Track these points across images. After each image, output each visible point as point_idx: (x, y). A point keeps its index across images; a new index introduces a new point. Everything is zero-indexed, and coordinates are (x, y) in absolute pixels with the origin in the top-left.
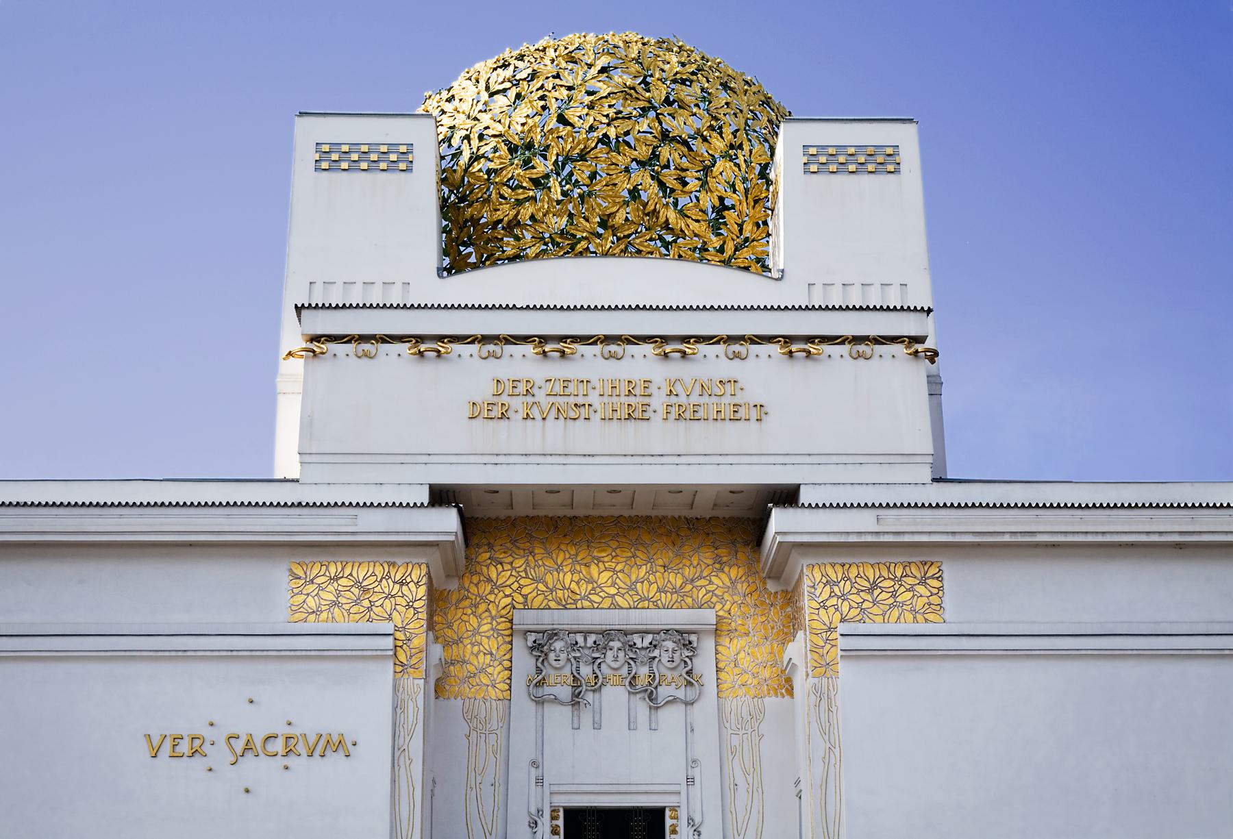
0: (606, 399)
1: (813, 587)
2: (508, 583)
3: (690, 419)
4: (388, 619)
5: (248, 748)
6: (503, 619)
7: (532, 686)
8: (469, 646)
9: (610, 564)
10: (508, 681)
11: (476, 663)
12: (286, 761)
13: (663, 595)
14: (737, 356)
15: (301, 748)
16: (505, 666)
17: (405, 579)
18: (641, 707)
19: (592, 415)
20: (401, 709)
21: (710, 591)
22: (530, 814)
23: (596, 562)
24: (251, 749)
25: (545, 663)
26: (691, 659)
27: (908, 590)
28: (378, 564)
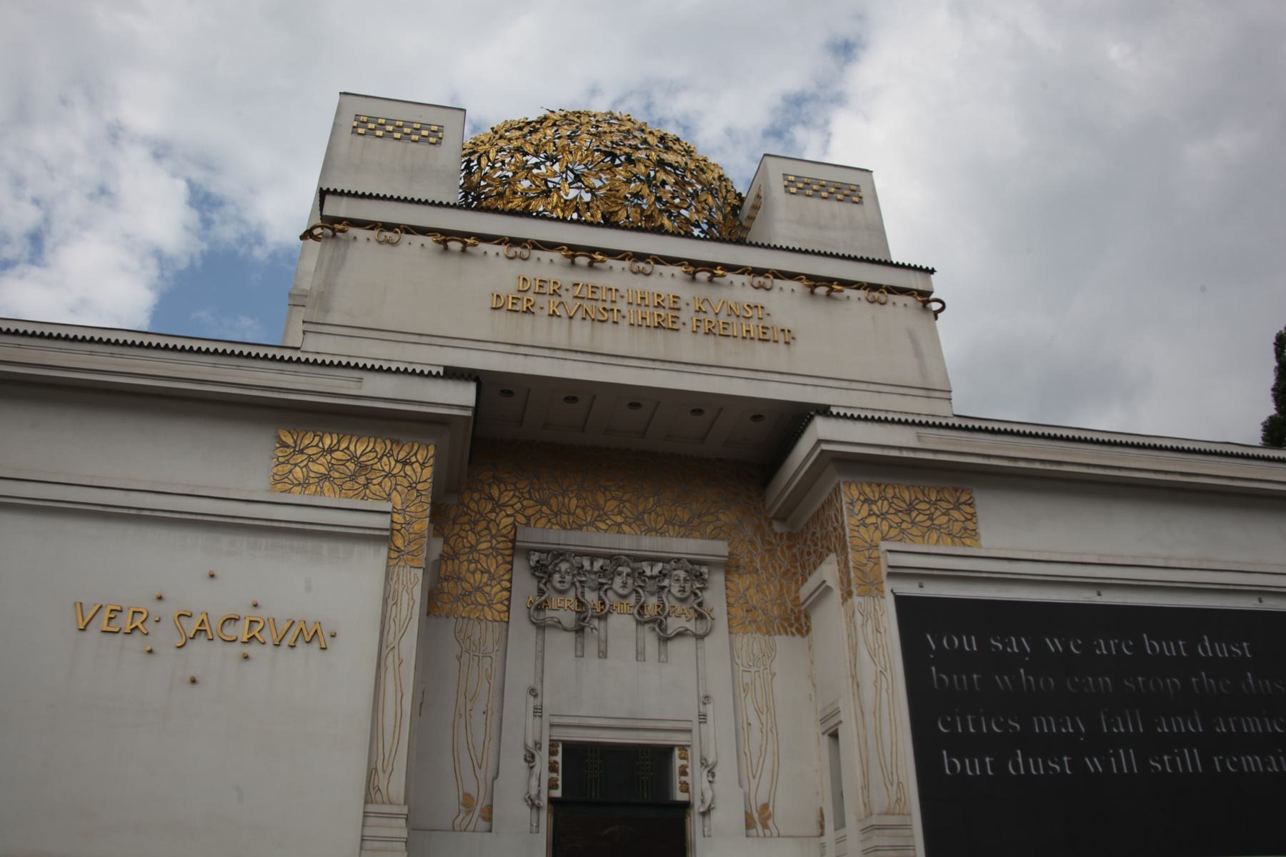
0: (634, 307)
1: (851, 504)
2: (510, 502)
3: (720, 335)
4: (385, 499)
6: (502, 539)
7: (532, 610)
8: (466, 563)
9: (617, 493)
10: (506, 603)
11: (472, 581)
13: (670, 527)
15: (267, 636)
16: (503, 586)
17: (409, 459)
18: (651, 641)
19: (620, 321)
20: (393, 600)
21: (717, 527)
22: (526, 746)
23: (602, 489)
24: (205, 631)
25: (548, 585)
26: (701, 592)
27: (944, 514)
28: (379, 440)
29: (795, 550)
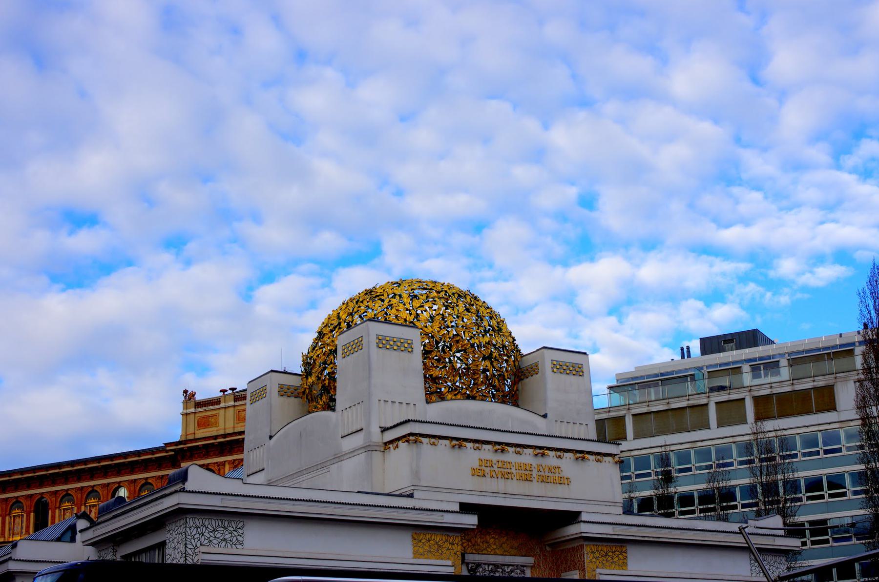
14: (560, 457)
29: (554, 558)
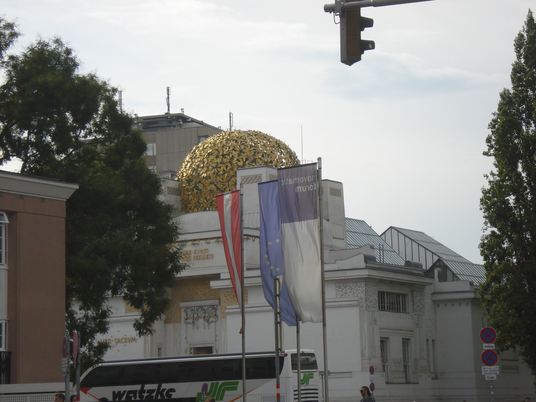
5: (119, 341)
12: (125, 344)
14: (208, 243)
18: (206, 324)
